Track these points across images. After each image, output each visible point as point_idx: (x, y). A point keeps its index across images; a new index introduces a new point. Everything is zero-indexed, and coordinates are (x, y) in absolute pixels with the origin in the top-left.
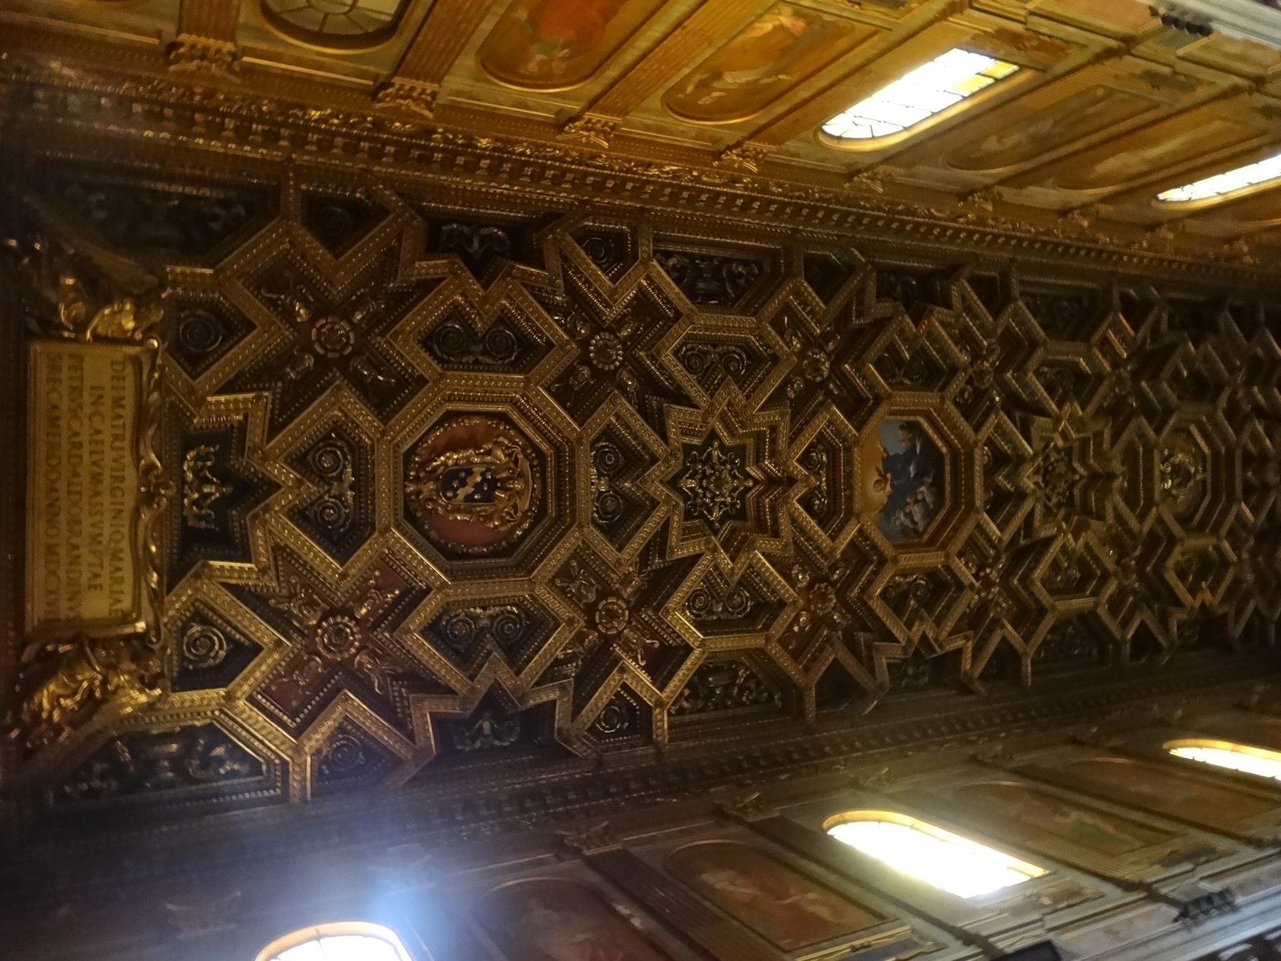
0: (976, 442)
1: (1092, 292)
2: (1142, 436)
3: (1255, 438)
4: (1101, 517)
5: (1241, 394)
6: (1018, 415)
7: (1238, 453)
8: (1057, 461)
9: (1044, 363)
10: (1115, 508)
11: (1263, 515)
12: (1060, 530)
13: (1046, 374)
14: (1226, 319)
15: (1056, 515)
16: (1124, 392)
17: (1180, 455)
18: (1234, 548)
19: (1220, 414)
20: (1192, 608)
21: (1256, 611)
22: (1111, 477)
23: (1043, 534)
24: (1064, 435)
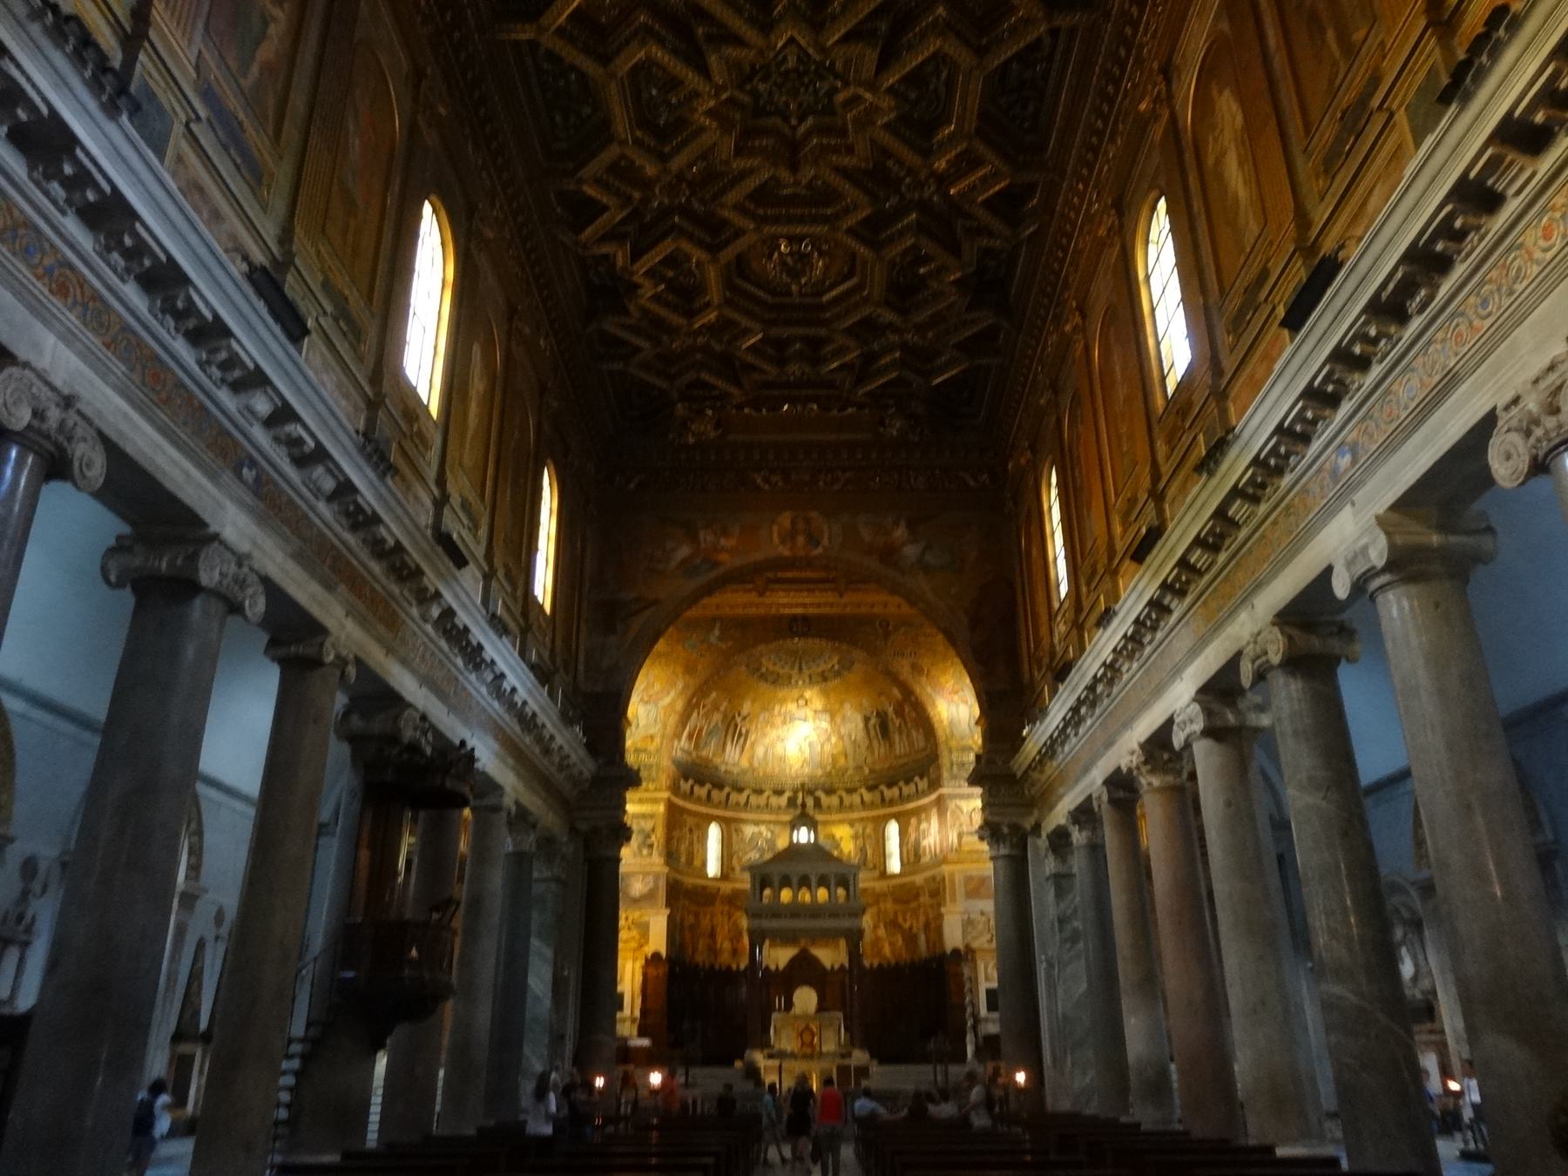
2: (847, 211)
4: (739, 151)
5: (894, 338)
6: (883, 26)
7: (823, 332)
8: (816, 91)
10: (751, 171)
11: (750, 359)
12: (719, 89)
15: (740, 87)
18: (710, 328)
19: (866, 311)
20: (632, 274)
21: (638, 350)
22: (794, 167)
23: (713, 60)
24: (856, 100)
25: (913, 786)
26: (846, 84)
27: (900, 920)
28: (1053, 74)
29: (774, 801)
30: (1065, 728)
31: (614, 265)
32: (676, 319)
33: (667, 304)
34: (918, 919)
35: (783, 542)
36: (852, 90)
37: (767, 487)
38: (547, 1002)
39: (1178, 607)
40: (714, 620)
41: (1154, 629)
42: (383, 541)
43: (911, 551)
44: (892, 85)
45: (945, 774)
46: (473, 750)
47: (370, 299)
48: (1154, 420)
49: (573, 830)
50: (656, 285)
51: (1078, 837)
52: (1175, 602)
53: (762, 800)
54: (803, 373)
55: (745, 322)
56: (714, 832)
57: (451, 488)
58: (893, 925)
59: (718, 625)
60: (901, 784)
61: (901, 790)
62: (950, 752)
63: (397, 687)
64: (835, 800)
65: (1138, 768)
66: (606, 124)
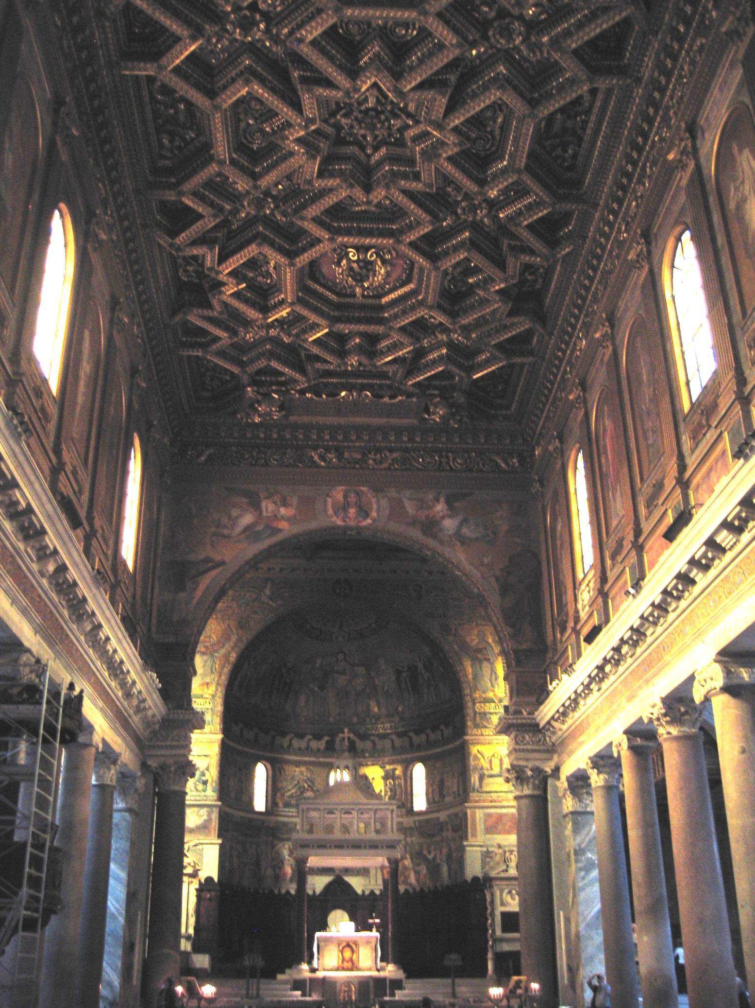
0: (425, 13)
1: (580, 182)
2: (411, 227)
3: (394, 347)
6: (453, 78)
7: (381, 329)
8: (389, 128)
9: (509, 115)
10: (331, 190)
11: (316, 350)
12: (312, 121)
13: (495, 121)
14: (522, 324)
15: (325, 121)
16: (459, 211)
17: (383, 271)
18: (280, 322)
19: (422, 313)
20: (218, 273)
21: (216, 339)
22: (368, 189)
23: (306, 100)
24: (425, 135)
25: (439, 733)
26: (417, 122)
27: (425, 852)
28: (591, 125)
29: (314, 744)
30: (590, 683)
31: (202, 265)
32: (252, 314)
33: (246, 301)
34: (441, 851)
35: (336, 513)
36: (422, 127)
37: (323, 464)
38: (122, 920)
39: (702, 579)
40: (266, 580)
41: (679, 598)
42: (17, 503)
43: (449, 524)
44: (457, 126)
45: (469, 724)
46: (82, 691)
47: (12, 289)
48: (680, 418)
49: (144, 766)
50: (238, 284)
51: (597, 780)
52: (700, 575)
53: (303, 744)
54: (360, 364)
55: (313, 318)
56: (261, 772)
57: (66, 457)
58: (418, 856)
59: (269, 586)
60: (428, 731)
61: (428, 735)
62: (474, 704)
63: (18, 634)
64: (368, 744)
65: (658, 719)
66: (207, 146)
